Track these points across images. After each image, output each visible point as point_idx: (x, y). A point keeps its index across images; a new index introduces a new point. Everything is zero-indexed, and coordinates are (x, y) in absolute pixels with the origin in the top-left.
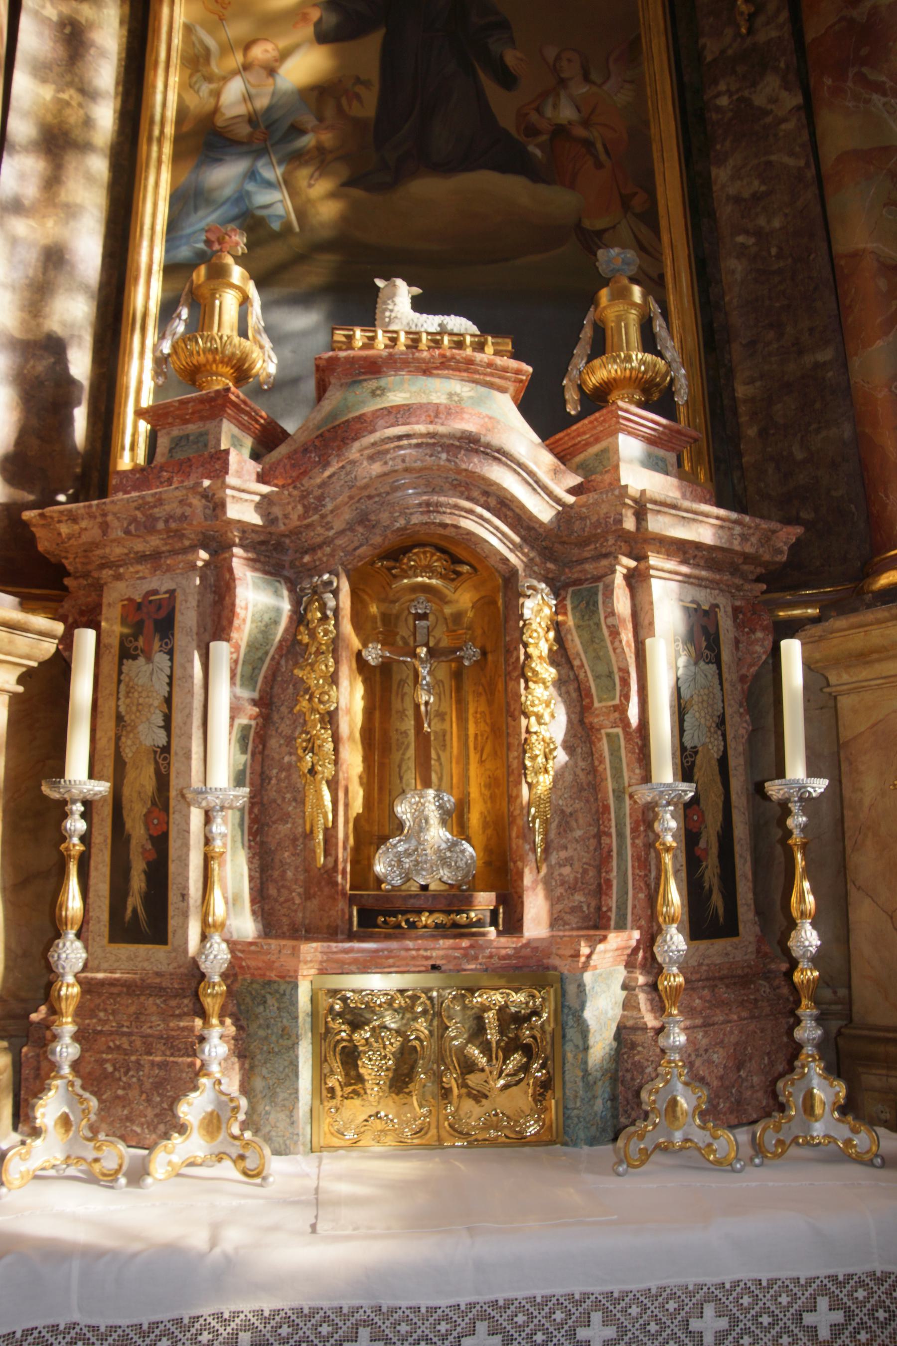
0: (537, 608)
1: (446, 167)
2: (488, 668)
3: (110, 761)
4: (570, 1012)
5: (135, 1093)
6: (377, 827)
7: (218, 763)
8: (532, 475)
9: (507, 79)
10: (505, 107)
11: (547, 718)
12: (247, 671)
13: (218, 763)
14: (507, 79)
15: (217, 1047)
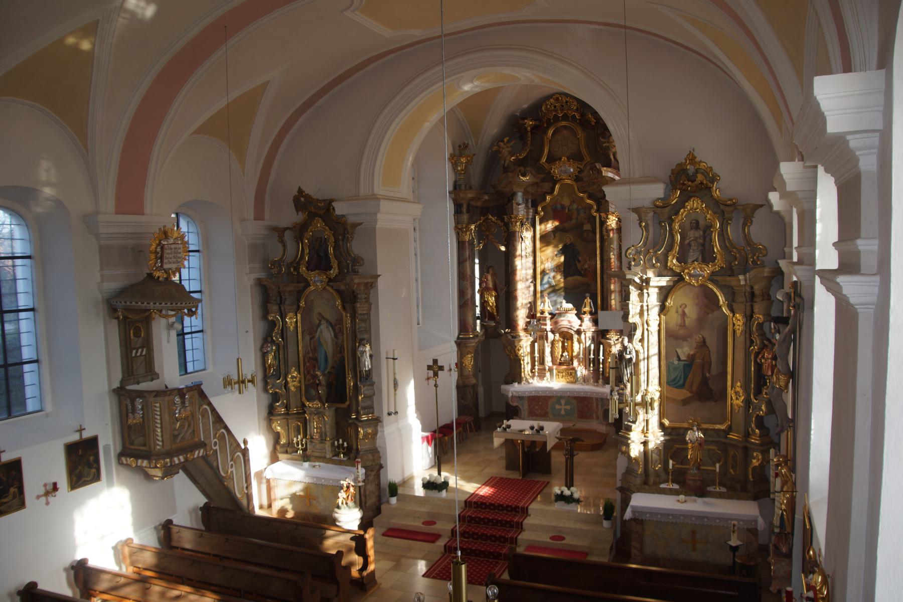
0: (576, 337)
1: (572, 276)
2: (572, 340)
3: (539, 353)
4: (576, 372)
5: (542, 376)
6: (562, 356)
7: (548, 350)
8: (576, 323)
9: (579, 262)
10: (579, 266)
11: (576, 346)
12: (550, 344)
13: (548, 350)
14: (579, 262)
15: (548, 374)
